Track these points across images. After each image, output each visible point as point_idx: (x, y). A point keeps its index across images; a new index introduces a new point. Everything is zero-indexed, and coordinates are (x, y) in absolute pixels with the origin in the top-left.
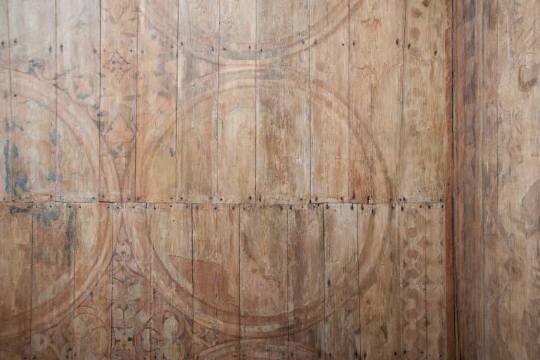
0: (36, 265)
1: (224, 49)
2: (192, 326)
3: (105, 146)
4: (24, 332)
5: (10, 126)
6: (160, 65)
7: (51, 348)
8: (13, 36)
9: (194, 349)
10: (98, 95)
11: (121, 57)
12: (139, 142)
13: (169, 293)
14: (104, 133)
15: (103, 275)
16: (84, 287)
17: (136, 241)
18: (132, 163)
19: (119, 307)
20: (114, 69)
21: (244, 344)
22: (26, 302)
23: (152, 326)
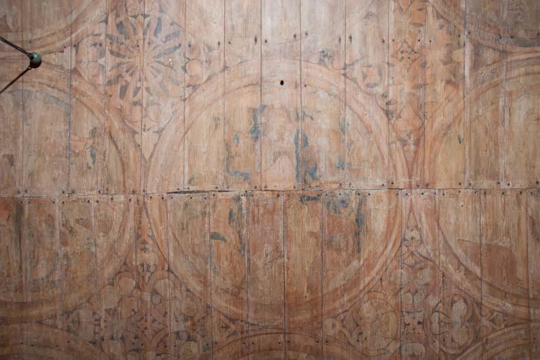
0: (327, 252)
1: (512, 37)
3: (394, 134)
4: (316, 317)
5: (300, 115)
6: (447, 54)
7: (343, 332)
8: (304, 30)
10: (386, 82)
11: (409, 47)
12: (427, 130)
13: (458, 277)
14: (392, 121)
15: (392, 261)
16: (373, 273)
17: (425, 227)
18: (421, 151)
19: (409, 291)
20: (403, 58)
21: (534, 327)
22: (317, 288)
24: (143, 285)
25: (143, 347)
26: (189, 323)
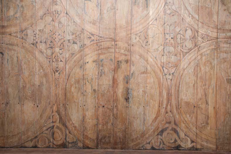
2: (198, 33)
9: (198, 43)
13: (188, 19)
19: (168, 25)
23: (181, 33)
24: (55, 20)
25: (54, 46)
26: (74, 36)
